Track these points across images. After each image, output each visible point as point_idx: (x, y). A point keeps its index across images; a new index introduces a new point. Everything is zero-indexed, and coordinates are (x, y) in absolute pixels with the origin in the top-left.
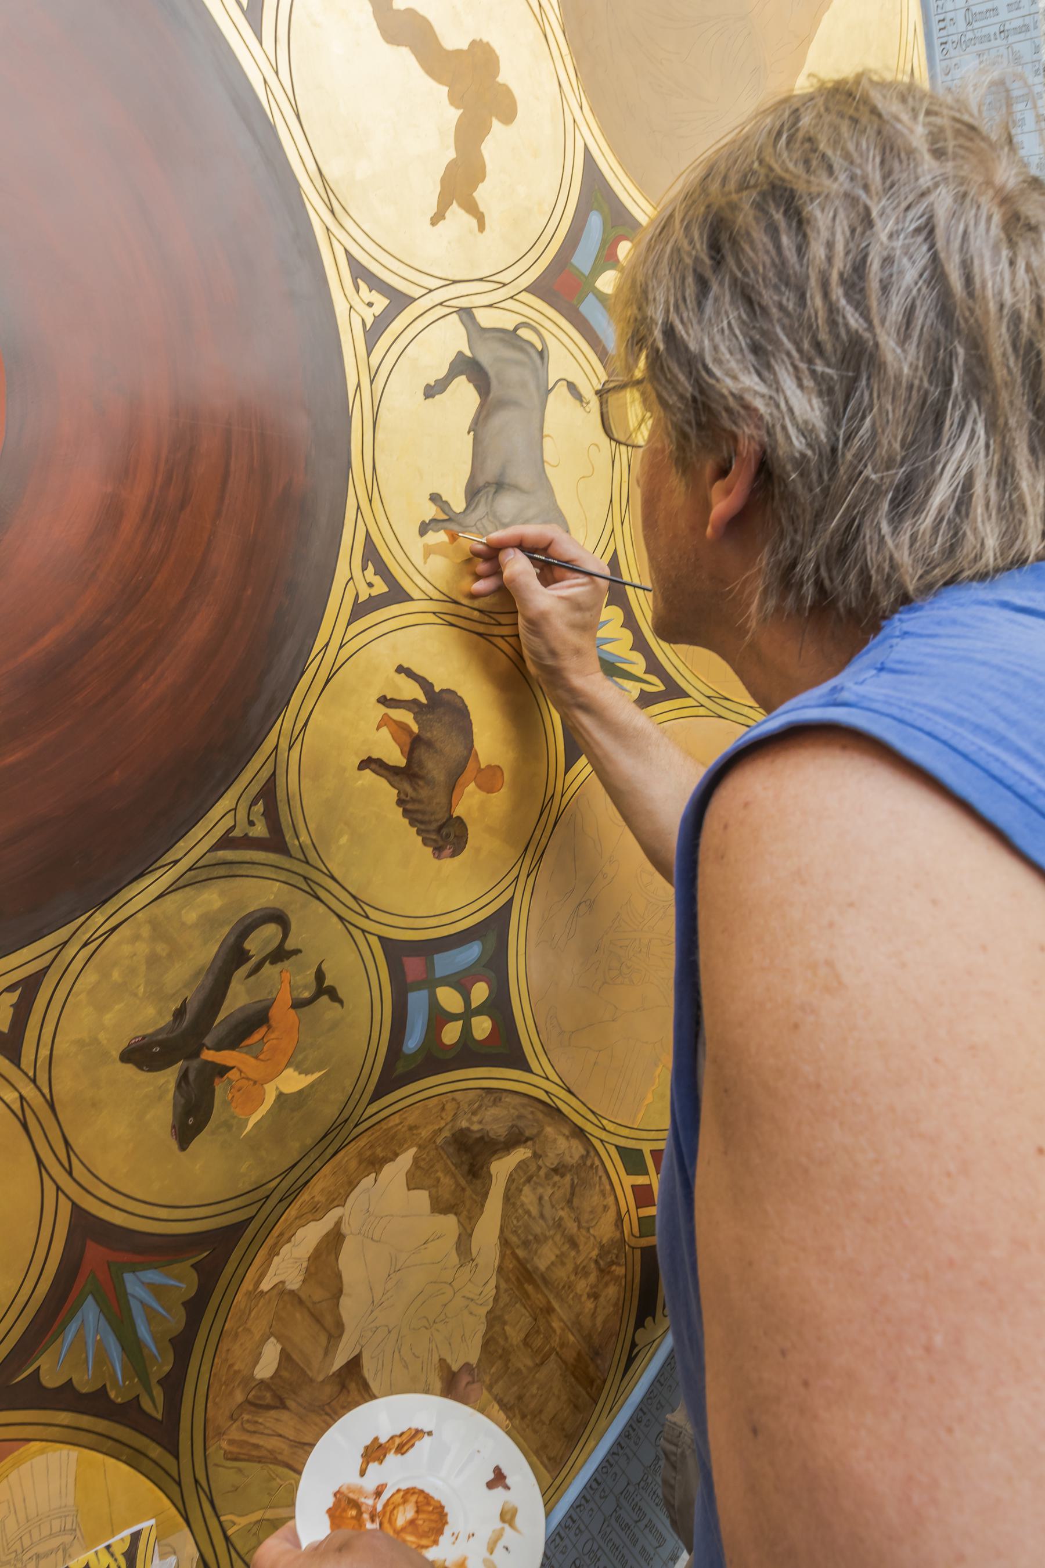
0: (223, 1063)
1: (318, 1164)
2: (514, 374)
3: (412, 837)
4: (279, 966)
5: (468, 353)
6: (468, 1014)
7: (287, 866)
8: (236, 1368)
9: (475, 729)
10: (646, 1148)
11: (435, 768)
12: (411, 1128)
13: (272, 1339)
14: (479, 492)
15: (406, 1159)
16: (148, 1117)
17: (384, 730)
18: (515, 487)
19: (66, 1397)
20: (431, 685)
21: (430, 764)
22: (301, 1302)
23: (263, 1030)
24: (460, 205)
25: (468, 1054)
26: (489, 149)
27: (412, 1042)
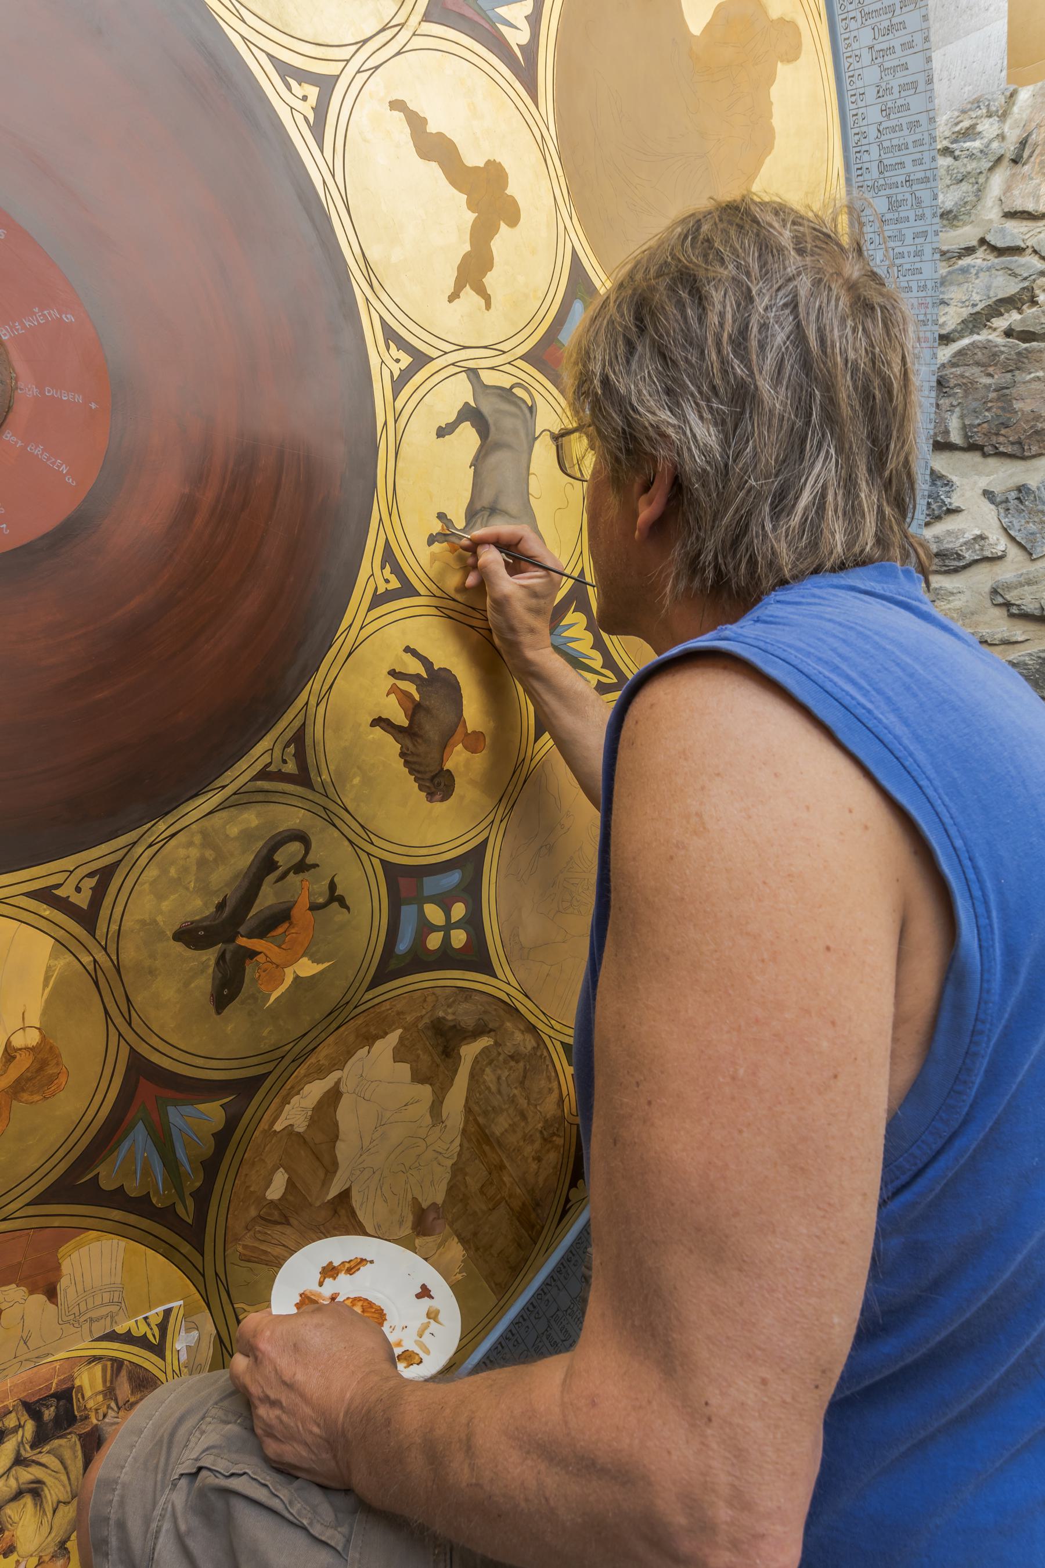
1: (323, 1035)
2: (508, 423)
3: (411, 784)
4: (301, 876)
5: (473, 404)
6: (448, 927)
7: (310, 798)
8: (252, 1189)
9: (464, 702)
11: (431, 730)
12: (399, 1013)
13: (281, 1169)
14: (476, 513)
15: (393, 1038)
16: (193, 985)
17: (393, 696)
18: (505, 513)
19: (118, 1199)
21: (427, 727)
22: (305, 1142)
23: (286, 925)
24: (472, 288)
25: (447, 958)
26: (498, 245)
27: (403, 946)
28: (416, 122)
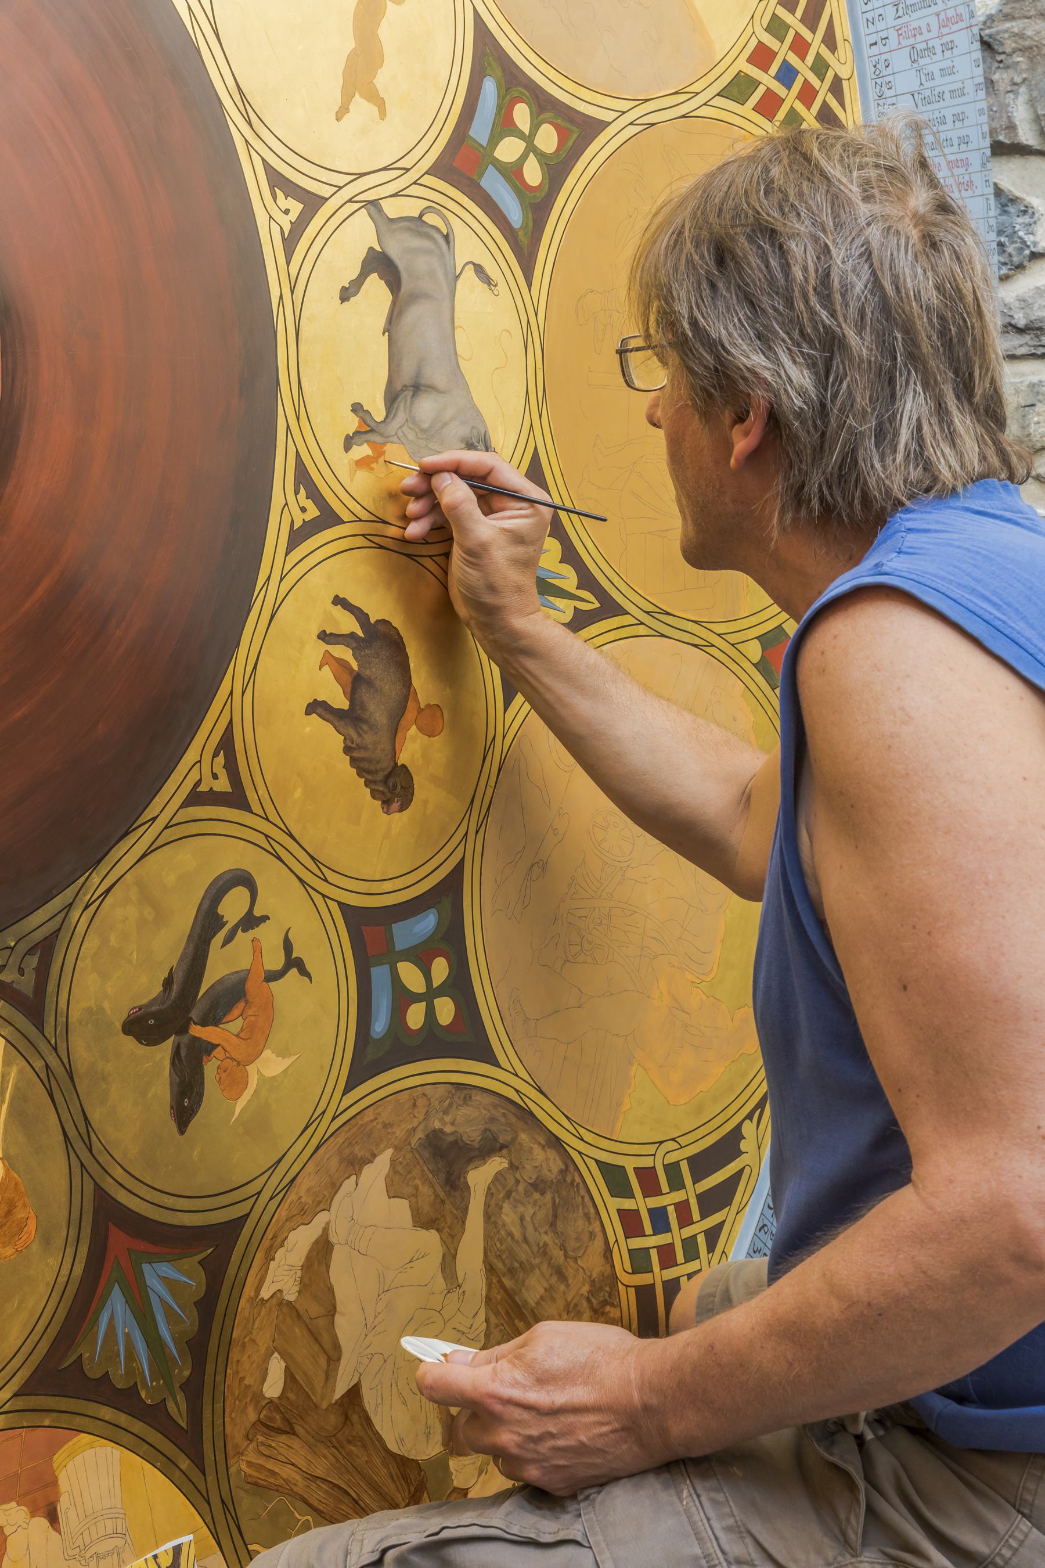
2: (422, 264)
5: (378, 249)
6: (430, 995)
8: (247, 1382)
9: (412, 665)
10: (630, 1165)
11: (377, 712)
12: (386, 1126)
15: (383, 1162)
16: (150, 1095)
17: (326, 668)
18: (432, 388)
20: (367, 616)
21: (372, 706)
22: (299, 1316)
23: (241, 1005)
24: (362, 96)
26: (386, 32)
27: (379, 1026)
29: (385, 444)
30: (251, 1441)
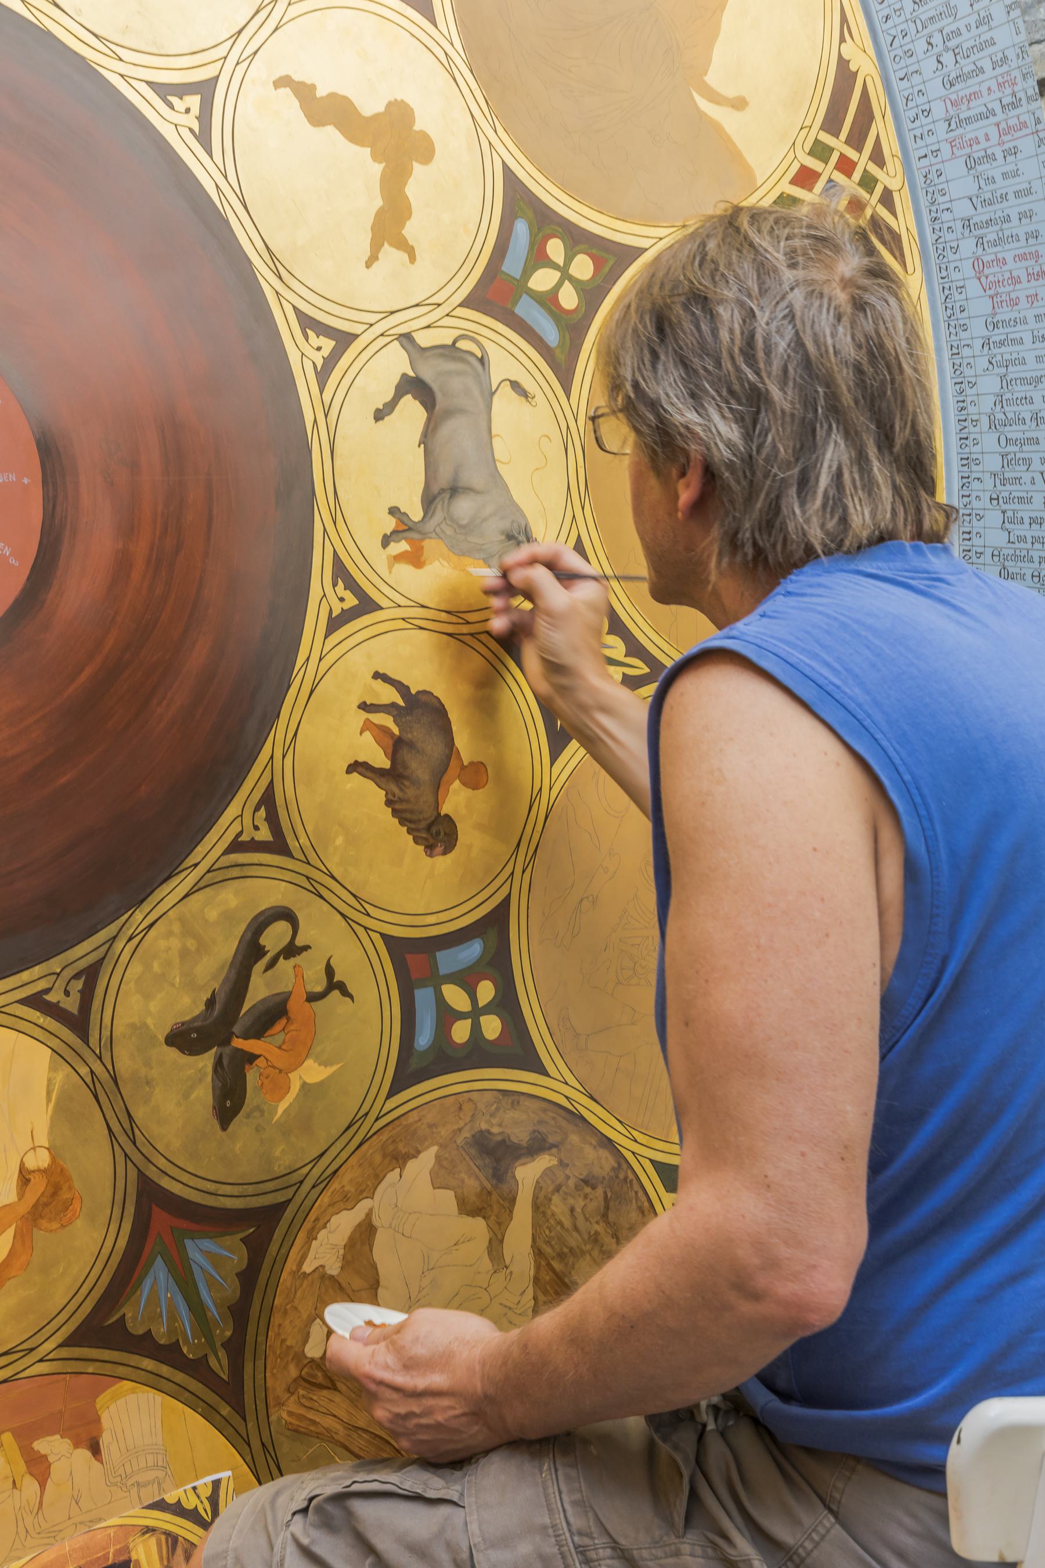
0: (251, 1051)
2: (456, 384)
4: (292, 961)
5: (412, 374)
6: (476, 1013)
8: (288, 1343)
9: (454, 729)
11: (419, 768)
14: (434, 498)
15: (428, 1157)
16: (193, 1097)
17: (367, 734)
18: (469, 490)
20: (408, 688)
21: (413, 765)
23: (283, 1021)
24: (391, 245)
25: (479, 1054)
26: (411, 190)
27: (424, 1039)
28: (304, 92)
29: (422, 540)
30: (292, 1394)
